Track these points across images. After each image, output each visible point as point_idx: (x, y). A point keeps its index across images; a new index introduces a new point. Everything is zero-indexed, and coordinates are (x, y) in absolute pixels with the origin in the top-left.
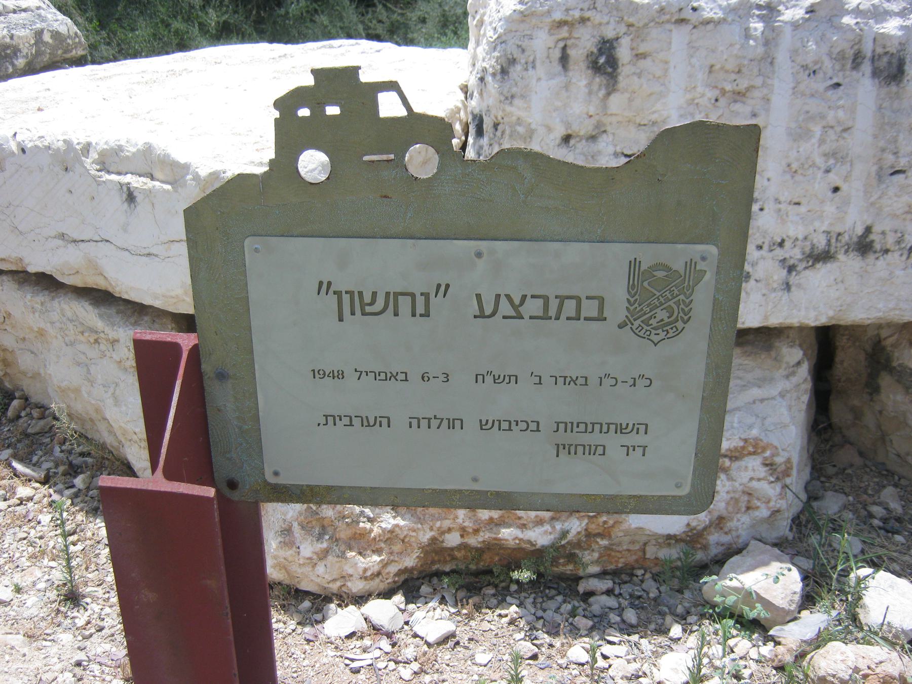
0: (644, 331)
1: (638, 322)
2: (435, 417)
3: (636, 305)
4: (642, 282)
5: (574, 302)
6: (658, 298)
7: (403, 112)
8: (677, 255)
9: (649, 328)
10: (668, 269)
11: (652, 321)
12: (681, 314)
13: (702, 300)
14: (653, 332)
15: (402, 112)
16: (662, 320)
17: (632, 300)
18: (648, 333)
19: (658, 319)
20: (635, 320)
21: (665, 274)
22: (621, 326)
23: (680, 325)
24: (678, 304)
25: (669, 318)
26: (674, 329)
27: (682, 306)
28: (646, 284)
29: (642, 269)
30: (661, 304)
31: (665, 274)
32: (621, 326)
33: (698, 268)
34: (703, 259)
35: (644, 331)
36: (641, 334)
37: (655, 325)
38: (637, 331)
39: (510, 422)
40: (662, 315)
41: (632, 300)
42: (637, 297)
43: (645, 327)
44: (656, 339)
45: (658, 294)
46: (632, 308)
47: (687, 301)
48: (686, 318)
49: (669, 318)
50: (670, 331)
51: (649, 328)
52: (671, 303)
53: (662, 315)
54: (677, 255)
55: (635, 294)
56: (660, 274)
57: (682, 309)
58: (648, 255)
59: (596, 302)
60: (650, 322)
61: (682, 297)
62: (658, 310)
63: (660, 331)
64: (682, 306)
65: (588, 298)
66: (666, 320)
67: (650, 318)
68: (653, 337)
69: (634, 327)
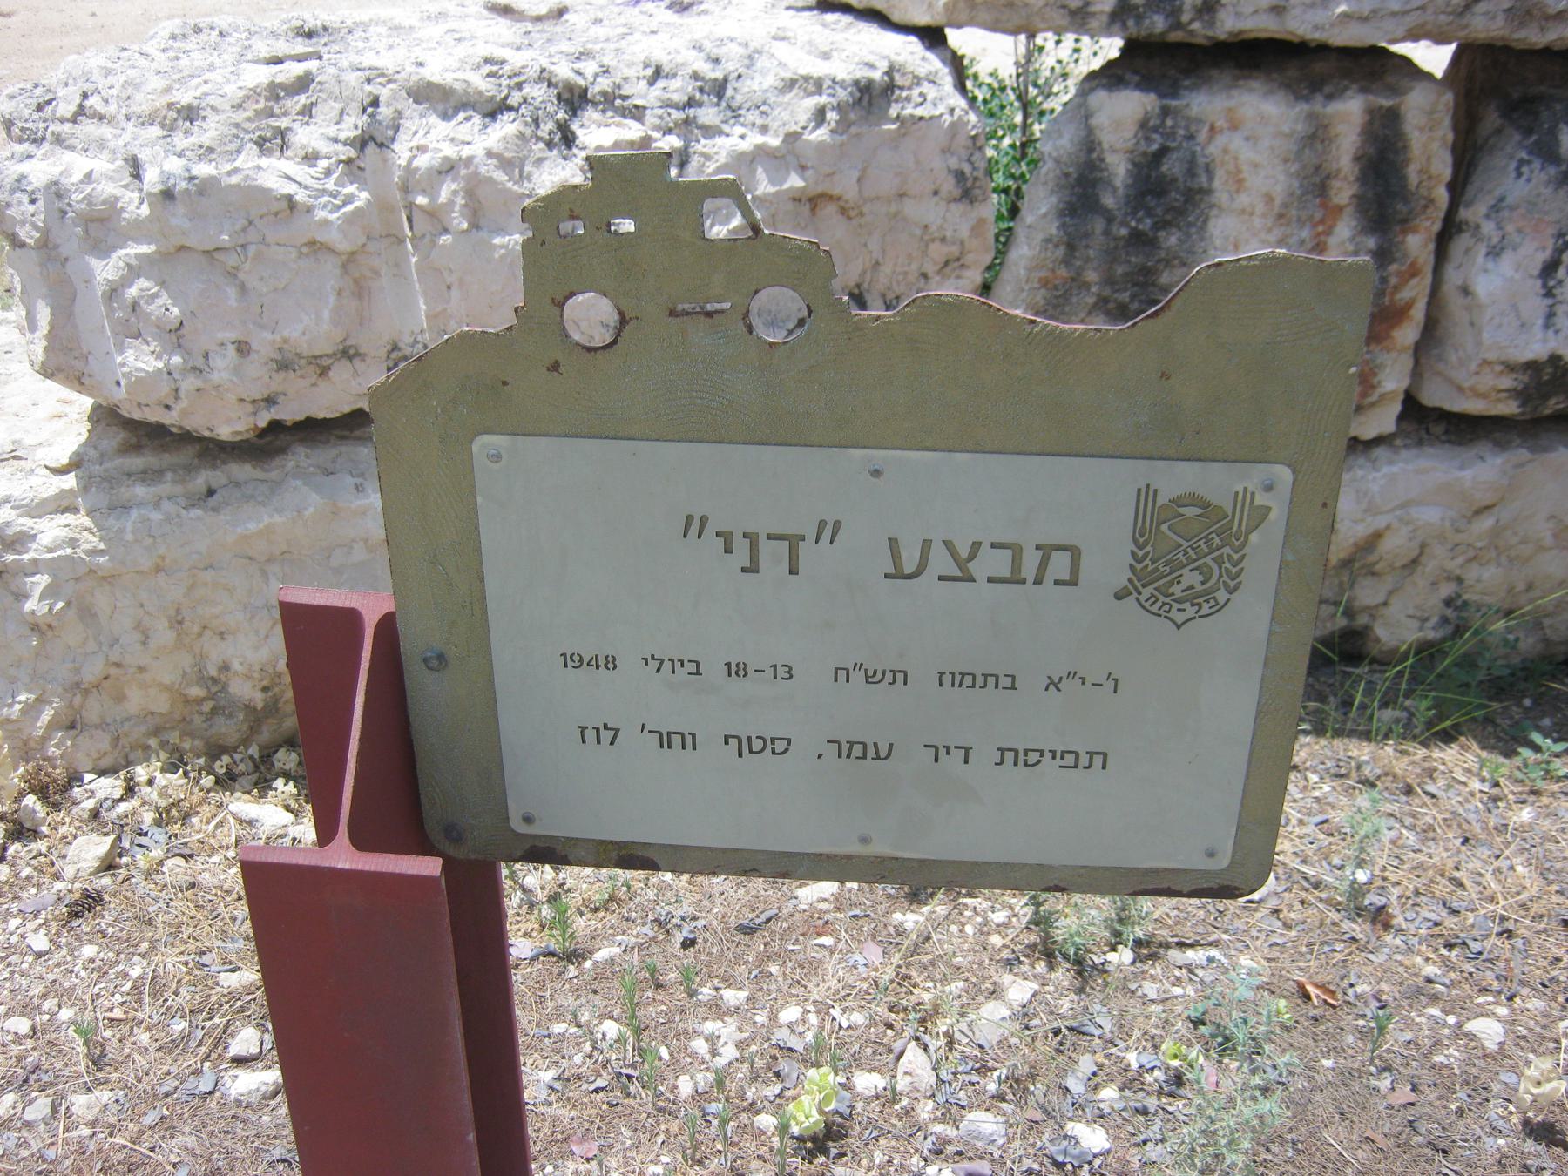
0: (1159, 604)
1: (1146, 592)
2: (606, 727)
3: (1147, 561)
6: (1186, 553)
9: (1167, 600)
10: (1205, 505)
11: (1176, 590)
12: (1225, 578)
13: (1264, 551)
14: (1176, 606)
16: (1192, 587)
18: (1166, 608)
19: (1184, 585)
20: (1144, 586)
21: (1199, 511)
22: (1119, 596)
23: (1222, 595)
24: (1219, 561)
25: (1203, 583)
26: (1212, 602)
27: (1227, 565)
28: (1164, 527)
29: (1159, 503)
31: (1199, 511)
32: (1119, 596)
33: (1258, 501)
34: (1269, 488)
35: (1159, 604)
36: (1155, 609)
37: (1178, 594)
38: (1147, 605)
40: (1191, 578)
41: (1140, 553)
42: (1149, 548)
44: (1180, 617)
46: (1139, 567)
47: (1236, 556)
48: (1232, 584)
49: (1203, 583)
50: (1206, 606)
51: (1167, 600)
52: (1208, 560)
53: (1191, 578)
55: (1146, 543)
57: (1228, 571)
59: (1009, 553)
60: (1171, 590)
62: (1185, 571)
63: (1186, 605)
65: (769, 537)
66: (1199, 587)
67: (1171, 583)
68: (1174, 614)
69: (1142, 598)
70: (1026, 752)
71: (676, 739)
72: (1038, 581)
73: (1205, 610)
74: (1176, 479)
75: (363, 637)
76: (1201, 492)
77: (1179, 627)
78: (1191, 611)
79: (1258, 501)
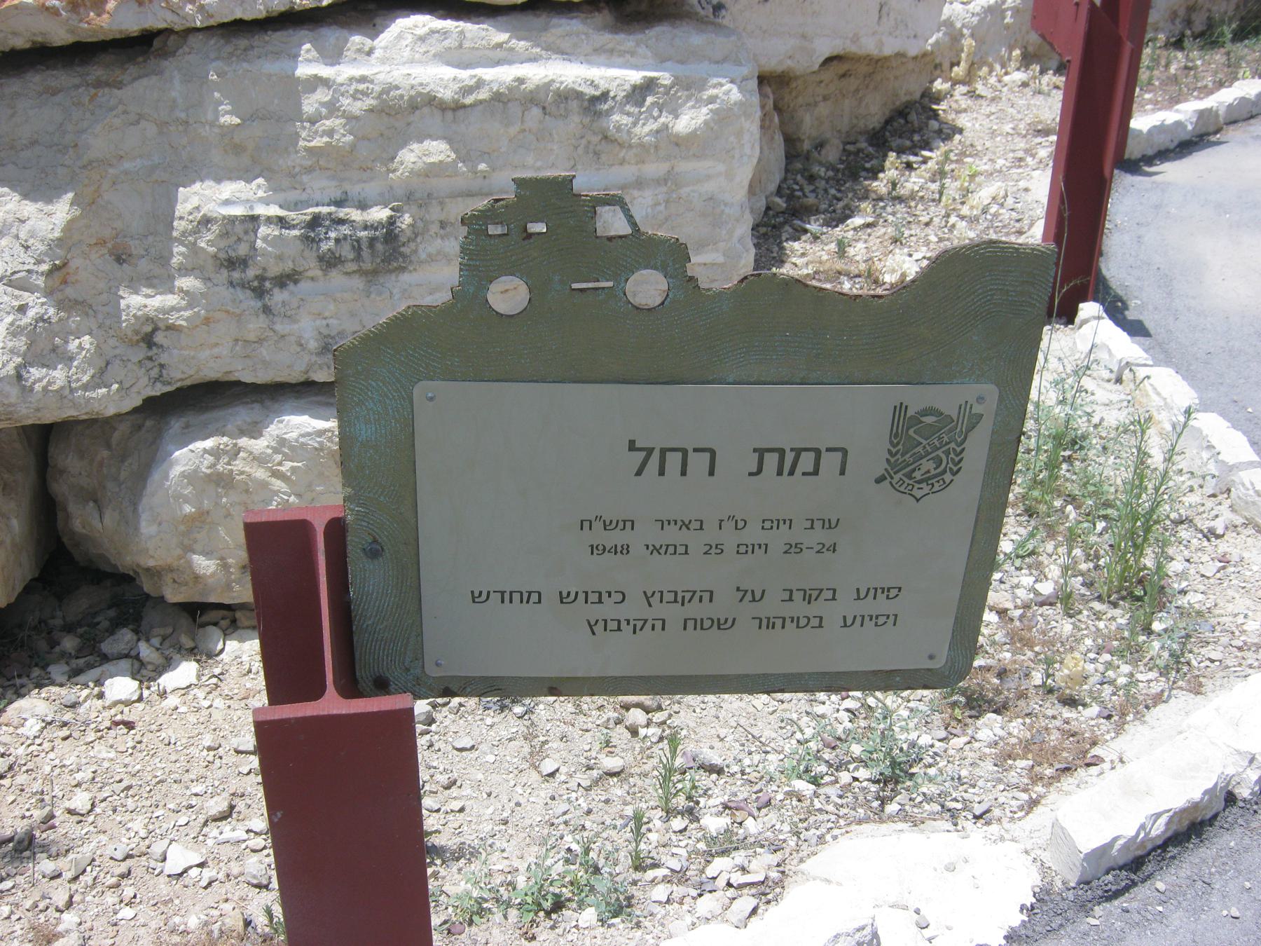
1: (900, 475)
3: (899, 456)
4: (908, 429)
5: (812, 455)
7: (627, 230)
8: (946, 398)
11: (918, 475)
12: (951, 465)
14: (917, 486)
15: (627, 230)
16: (928, 472)
17: (894, 451)
19: (922, 471)
22: (879, 480)
23: (948, 477)
24: (947, 453)
27: (952, 455)
28: (911, 432)
29: (908, 415)
30: (928, 454)
32: (879, 480)
33: (974, 411)
34: (980, 399)
36: (902, 489)
37: (919, 478)
39: (600, 593)
42: (900, 447)
43: (907, 481)
44: (918, 494)
45: (925, 442)
46: (892, 460)
47: (959, 449)
48: (955, 469)
50: (936, 485)
52: (940, 453)
53: (928, 465)
54: (946, 398)
55: (898, 443)
56: (929, 420)
58: (917, 397)
61: (953, 445)
63: (923, 485)
64: (952, 455)
66: (933, 472)
67: (914, 470)
69: (894, 482)
70: (889, 590)
71: (516, 597)
72: (791, 473)
73: (937, 488)
74: (917, 397)
75: (315, 536)
76: (936, 406)
77: (918, 501)
78: (926, 489)
79: (974, 411)
